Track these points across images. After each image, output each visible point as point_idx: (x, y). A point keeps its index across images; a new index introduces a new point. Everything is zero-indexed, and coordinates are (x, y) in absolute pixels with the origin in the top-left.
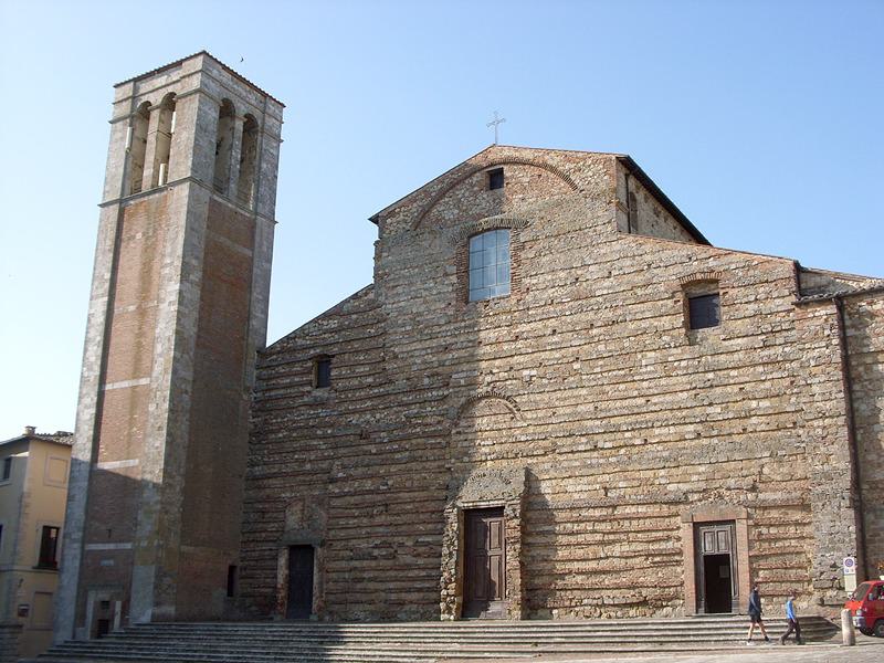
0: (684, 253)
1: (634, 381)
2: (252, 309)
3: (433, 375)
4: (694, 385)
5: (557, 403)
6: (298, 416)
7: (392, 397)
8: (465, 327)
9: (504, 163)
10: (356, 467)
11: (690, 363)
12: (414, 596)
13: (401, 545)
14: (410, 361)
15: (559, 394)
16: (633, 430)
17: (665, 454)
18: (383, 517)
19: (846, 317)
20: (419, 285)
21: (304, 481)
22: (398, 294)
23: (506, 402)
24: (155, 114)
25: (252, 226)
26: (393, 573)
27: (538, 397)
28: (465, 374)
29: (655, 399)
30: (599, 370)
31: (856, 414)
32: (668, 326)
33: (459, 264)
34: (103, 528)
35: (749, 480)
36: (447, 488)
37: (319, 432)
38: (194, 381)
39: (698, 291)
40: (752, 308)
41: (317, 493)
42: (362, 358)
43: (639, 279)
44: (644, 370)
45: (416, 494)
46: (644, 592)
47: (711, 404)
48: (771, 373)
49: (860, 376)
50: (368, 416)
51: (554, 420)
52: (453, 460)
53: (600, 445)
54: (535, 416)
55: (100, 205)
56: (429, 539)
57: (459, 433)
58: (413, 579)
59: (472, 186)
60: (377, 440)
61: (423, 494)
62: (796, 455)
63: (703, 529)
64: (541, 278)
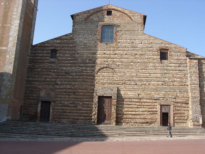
0: (161, 42)
1: (147, 70)
3: (90, 60)
5: (126, 72)
6: (45, 65)
7: (77, 64)
9: (112, 10)
10: (65, 81)
12: (82, 118)
13: (79, 104)
15: (127, 70)
16: (146, 81)
17: (154, 88)
18: (73, 96)
20: (86, 36)
25: (33, 10)
26: (75, 111)
27: (121, 70)
29: (152, 75)
30: (138, 65)
32: (156, 58)
35: (174, 96)
37: (52, 70)
39: (163, 51)
40: (176, 58)
42: (67, 52)
43: (149, 45)
44: (150, 67)
45: (83, 91)
46: (147, 120)
47: (165, 78)
50: (69, 68)
51: (125, 76)
53: (137, 84)
54: (120, 74)
63: (162, 107)
64: (123, 40)
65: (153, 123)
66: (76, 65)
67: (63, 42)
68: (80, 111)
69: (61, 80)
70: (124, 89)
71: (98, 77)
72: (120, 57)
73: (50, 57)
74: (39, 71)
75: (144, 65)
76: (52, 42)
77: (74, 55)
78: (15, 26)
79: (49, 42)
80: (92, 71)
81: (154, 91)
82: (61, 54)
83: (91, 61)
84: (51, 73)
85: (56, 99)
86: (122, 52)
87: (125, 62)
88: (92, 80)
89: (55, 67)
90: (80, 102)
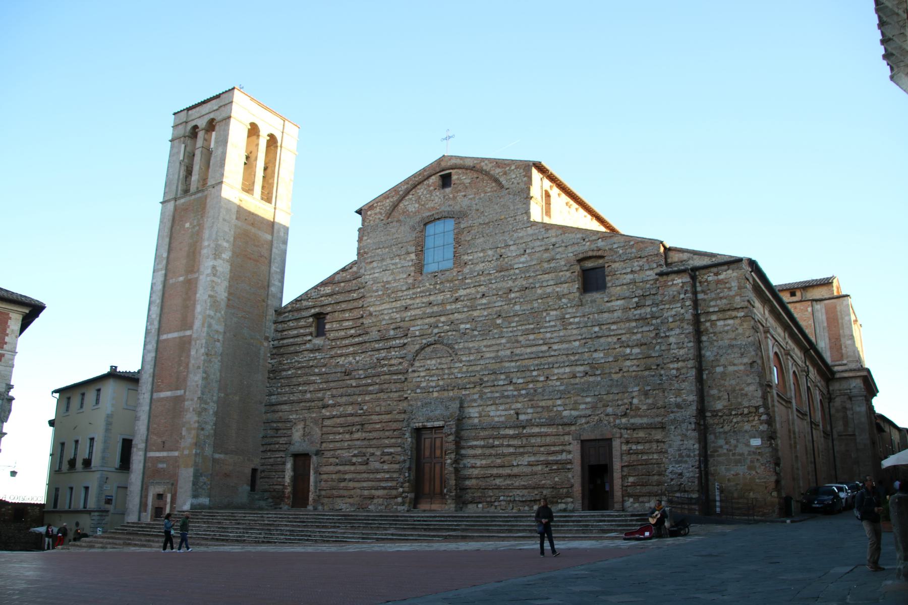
1: (540, 333)
2: (271, 279)
4: (584, 336)
5: (484, 349)
6: (302, 358)
7: (368, 344)
8: (420, 292)
9: (452, 169)
10: (341, 396)
11: (582, 319)
12: (380, 493)
13: (373, 454)
14: (381, 317)
15: (485, 343)
16: (538, 369)
17: (562, 388)
19: (698, 284)
20: (389, 261)
21: (306, 406)
22: (373, 268)
23: (445, 348)
24: (201, 134)
26: (365, 475)
27: (471, 345)
28: (418, 328)
29: (555, 347)
30: (514, 324)
31: (703, 359)
32: (566, 291)
33: (417, 245)
34: (159, 440)
36: (405, 412)
37: (317, 370)
38: (225, 333)
39: (589, 264)
41: (314, 415)
42: (347, 315)
44: (548, 325)
45: (383, 416)
46: (545, 492)
47: (596, 351)
48: (642, 327)
49: (707, 330)
50: (351, 358)
52: (409, 392)
53: (514, 381)
54: (468, 359)
55: (161, 203)
56: (392, 450)
57: (414, 371)
58: (380, 480)
59: (429, 186)
60: (357, 376)
61: (386, 417)
62: (658, 389)
65: (563, 501)
66: (366, 348)
67: (337, 289)
68: (375, 475)
69: (334, 392)
70: (479, 402)
71: (416, 374)
72: (468, 307)
73: (314, 335)
74: (290, 376)
75: (531, 321)
76: (316, 293)
77: (361, 321)
78: (208, 275)
79: (309, 296)
80: (401, 360)
81: (560, 398)
82: (334, 323)
83: (399, 330)
84: (314, 378)
85: (324, 445)
86: (473, 291)
87: (481, 319)
88: (402, 384)
89: (322, 361)
90: (375, 449)
